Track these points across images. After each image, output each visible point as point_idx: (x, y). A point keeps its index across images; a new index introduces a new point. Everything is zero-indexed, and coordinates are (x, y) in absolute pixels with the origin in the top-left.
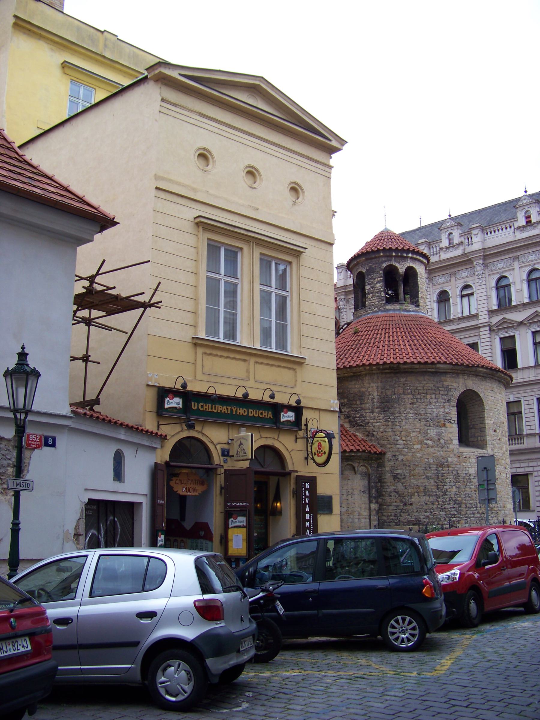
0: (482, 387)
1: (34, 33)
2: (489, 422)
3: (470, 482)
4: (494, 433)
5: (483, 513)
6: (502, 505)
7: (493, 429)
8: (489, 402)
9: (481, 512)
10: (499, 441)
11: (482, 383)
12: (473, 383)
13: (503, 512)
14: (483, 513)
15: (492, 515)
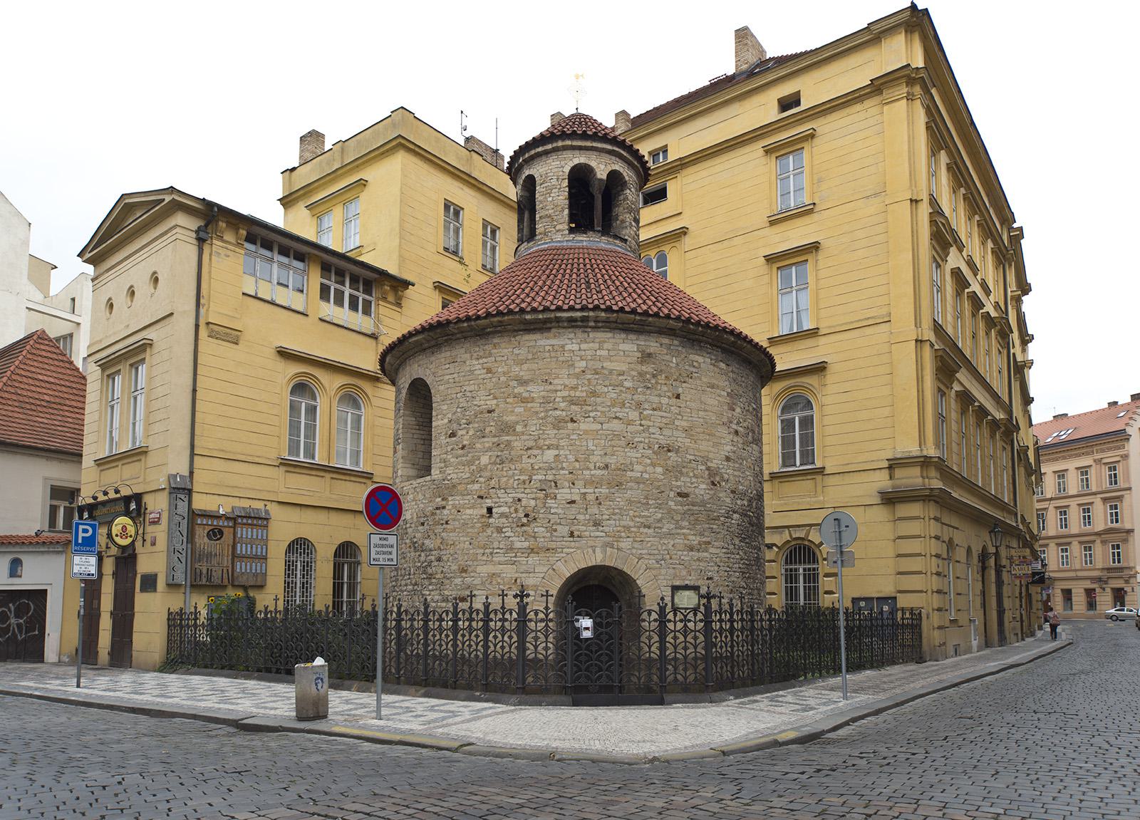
0: (431, 367)
1: (294, 200)
2: (440, 423)
3: (407, 533)
4: (448, 440)
5: (416, 584)
6: (454, 567)
7: (446, 434)
8: (442, 388)
9: (413, 582)
10: (460, 452)
11: (433, 358)
12: (419, 366)
13: (458, 581)
14: (416, 584)
15: (431, 587)
